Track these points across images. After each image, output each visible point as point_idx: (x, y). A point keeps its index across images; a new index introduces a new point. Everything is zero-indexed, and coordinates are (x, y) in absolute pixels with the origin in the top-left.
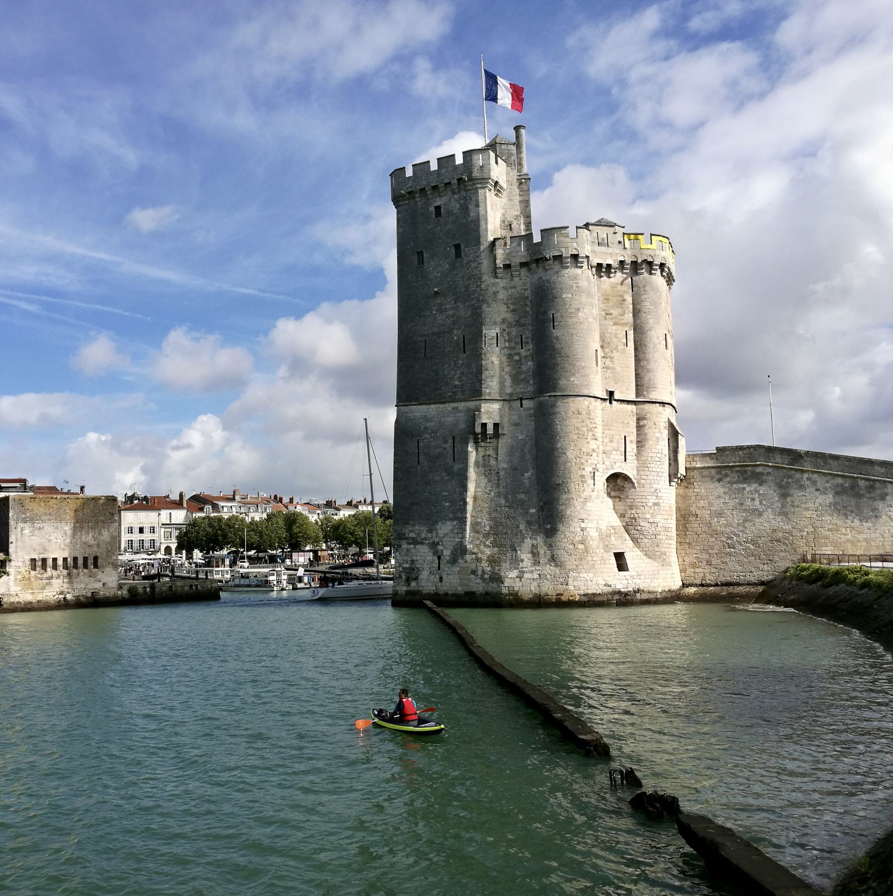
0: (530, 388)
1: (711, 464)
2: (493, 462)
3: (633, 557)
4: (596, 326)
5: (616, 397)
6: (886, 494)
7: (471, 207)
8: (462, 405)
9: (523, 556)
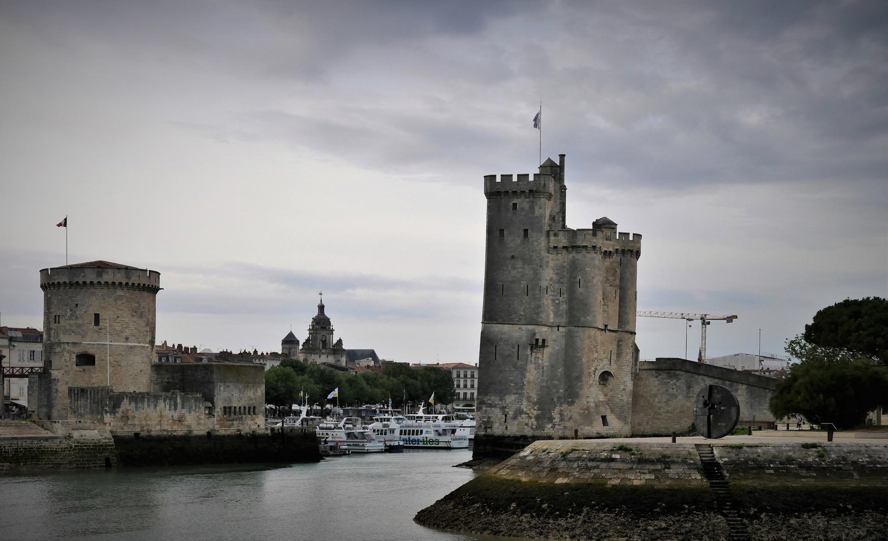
0: (564, 320)
1: (653, 367)
2: (540, 362)
3: (611, 418)
4: (601, 287)
8: (524, 327)
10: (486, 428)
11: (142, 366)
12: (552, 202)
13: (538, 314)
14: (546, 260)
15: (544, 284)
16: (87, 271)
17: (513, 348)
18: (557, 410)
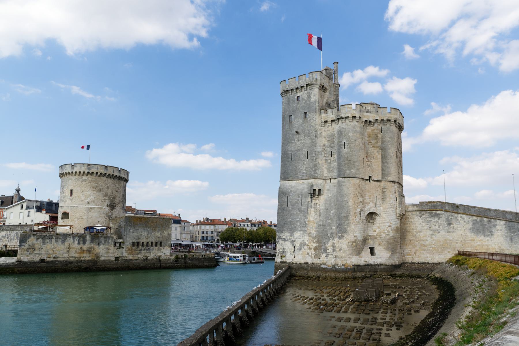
0: (335, 174)
1: (417, 209)
2: (318, 206)
5: (373, 178)
6: (496, 225)
7: (312, 96)
8: (306, 181)
9: (329, 248)
11: (100, 219)
12: (327, 94)
13: (315, 171)
14: (319, 132)
15: (319, 149)
16: (67, 166)
17: (299, 197)
18: (331, 242)
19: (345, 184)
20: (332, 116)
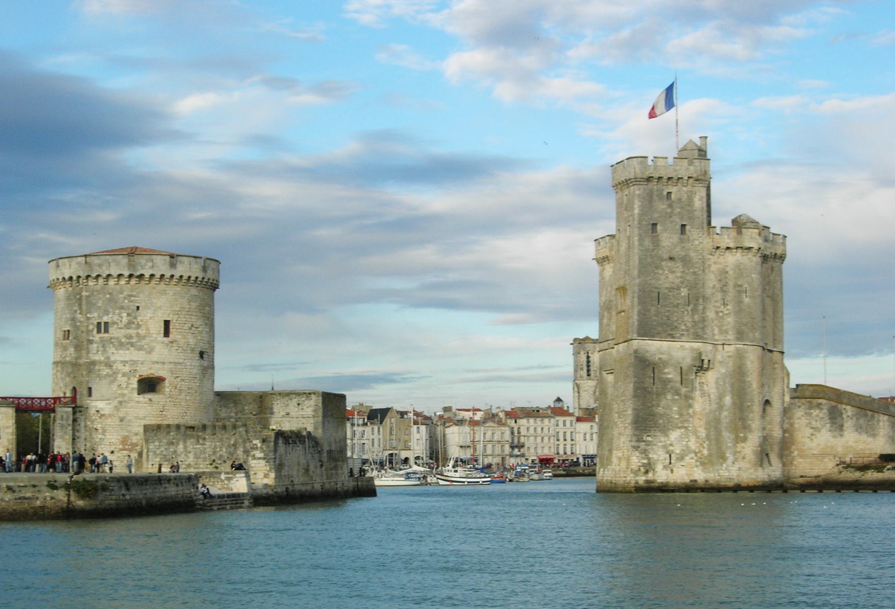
0: (729, 337)
2: (705, 387)
8: (687, 345)
10: (647, 472)
15: (709, 292)
19: (748, 355)
20: (728, 241)
